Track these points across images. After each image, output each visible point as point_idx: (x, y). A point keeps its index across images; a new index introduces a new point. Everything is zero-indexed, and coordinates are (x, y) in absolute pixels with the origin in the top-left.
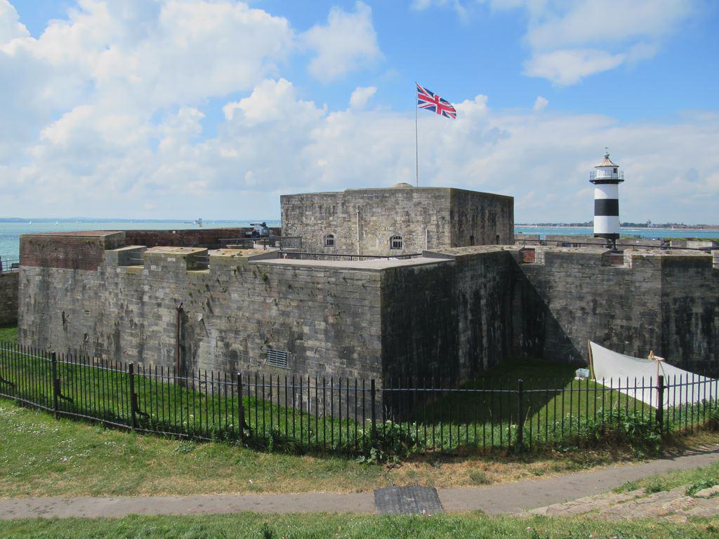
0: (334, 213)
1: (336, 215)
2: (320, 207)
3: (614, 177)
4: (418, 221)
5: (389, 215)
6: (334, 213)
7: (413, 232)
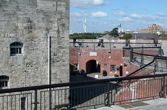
4: (40, 28)
5: (9, 21)
7: (36, 38)
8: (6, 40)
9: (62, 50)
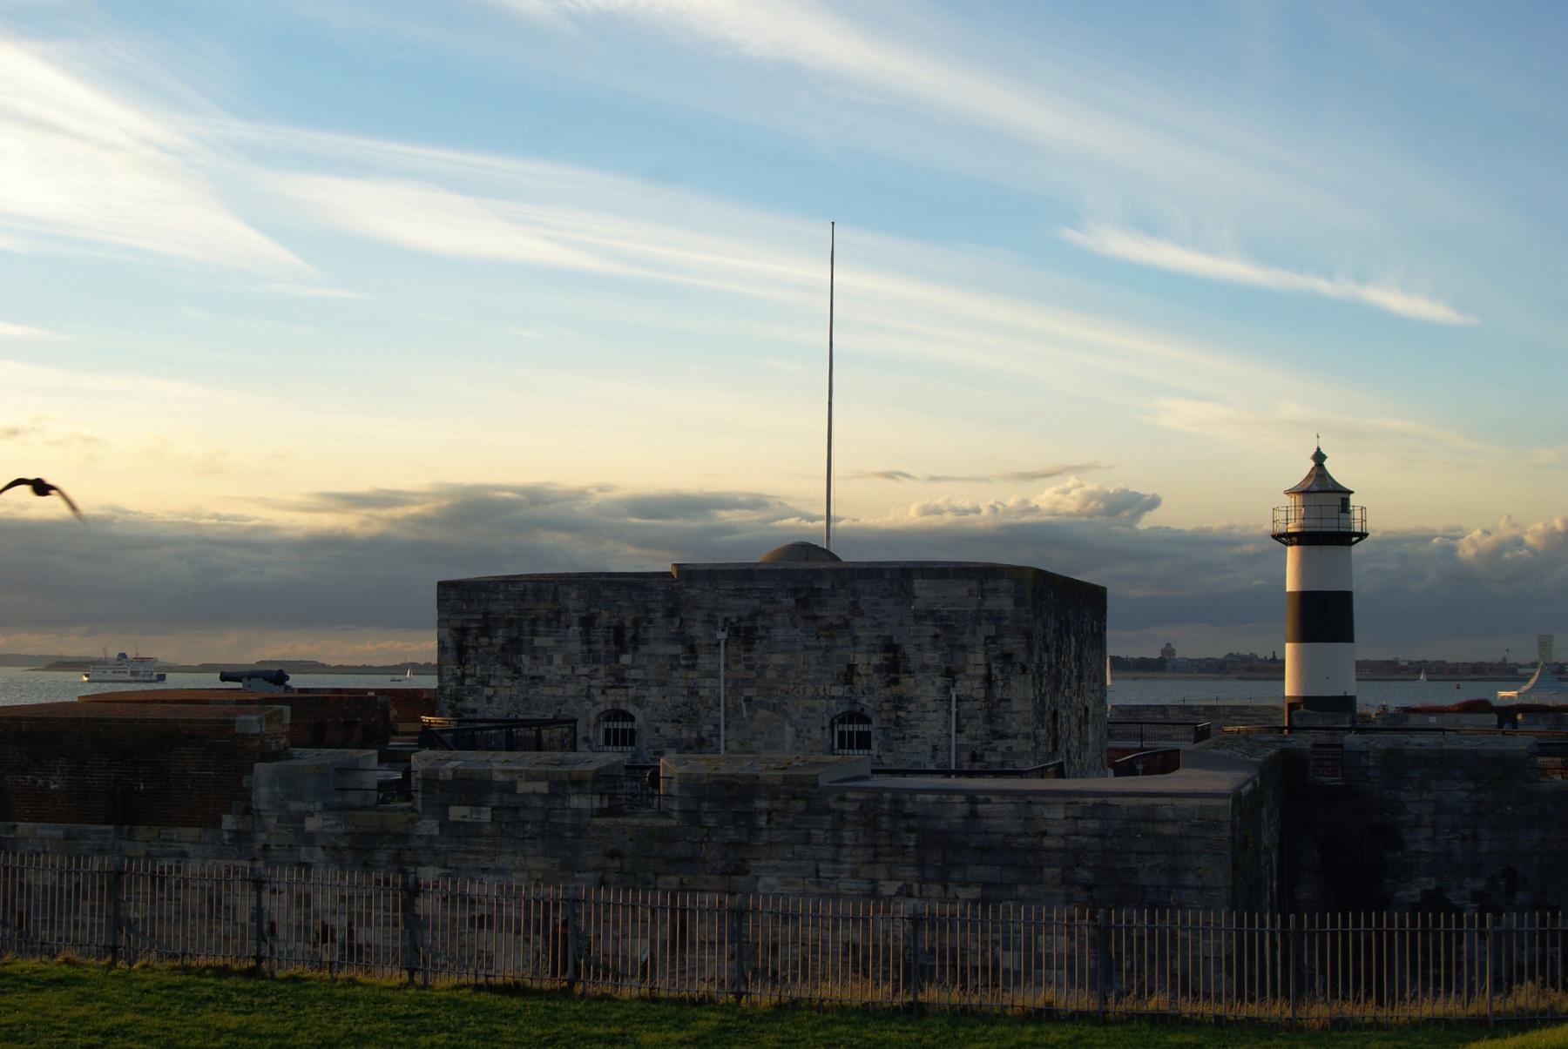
0: (636, 641)
1: (643, 649)
2: (587, 622)
3: (1330, 526)
4: (925, 668)
5: (828, 650)
6: (634, 639)
7: (910, 700)
8: (821, 705)
9: (1002, 745)
